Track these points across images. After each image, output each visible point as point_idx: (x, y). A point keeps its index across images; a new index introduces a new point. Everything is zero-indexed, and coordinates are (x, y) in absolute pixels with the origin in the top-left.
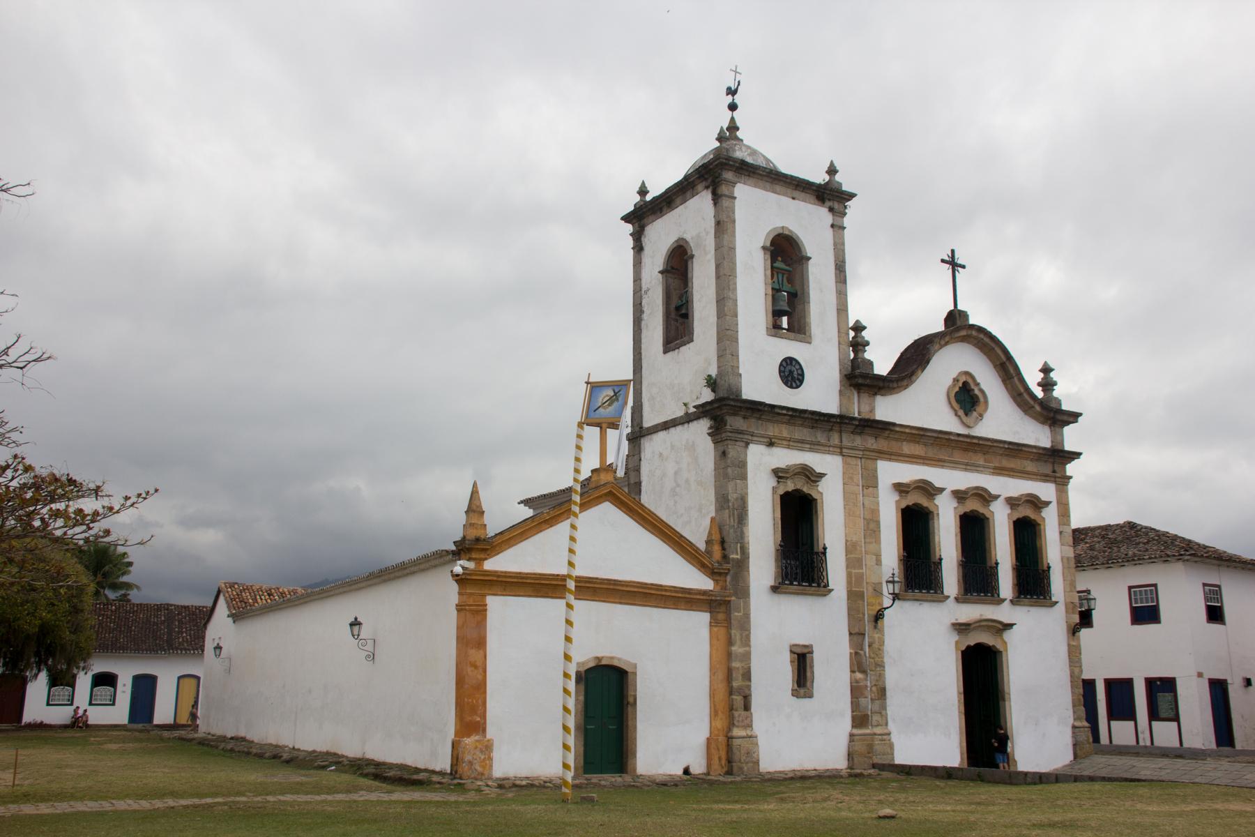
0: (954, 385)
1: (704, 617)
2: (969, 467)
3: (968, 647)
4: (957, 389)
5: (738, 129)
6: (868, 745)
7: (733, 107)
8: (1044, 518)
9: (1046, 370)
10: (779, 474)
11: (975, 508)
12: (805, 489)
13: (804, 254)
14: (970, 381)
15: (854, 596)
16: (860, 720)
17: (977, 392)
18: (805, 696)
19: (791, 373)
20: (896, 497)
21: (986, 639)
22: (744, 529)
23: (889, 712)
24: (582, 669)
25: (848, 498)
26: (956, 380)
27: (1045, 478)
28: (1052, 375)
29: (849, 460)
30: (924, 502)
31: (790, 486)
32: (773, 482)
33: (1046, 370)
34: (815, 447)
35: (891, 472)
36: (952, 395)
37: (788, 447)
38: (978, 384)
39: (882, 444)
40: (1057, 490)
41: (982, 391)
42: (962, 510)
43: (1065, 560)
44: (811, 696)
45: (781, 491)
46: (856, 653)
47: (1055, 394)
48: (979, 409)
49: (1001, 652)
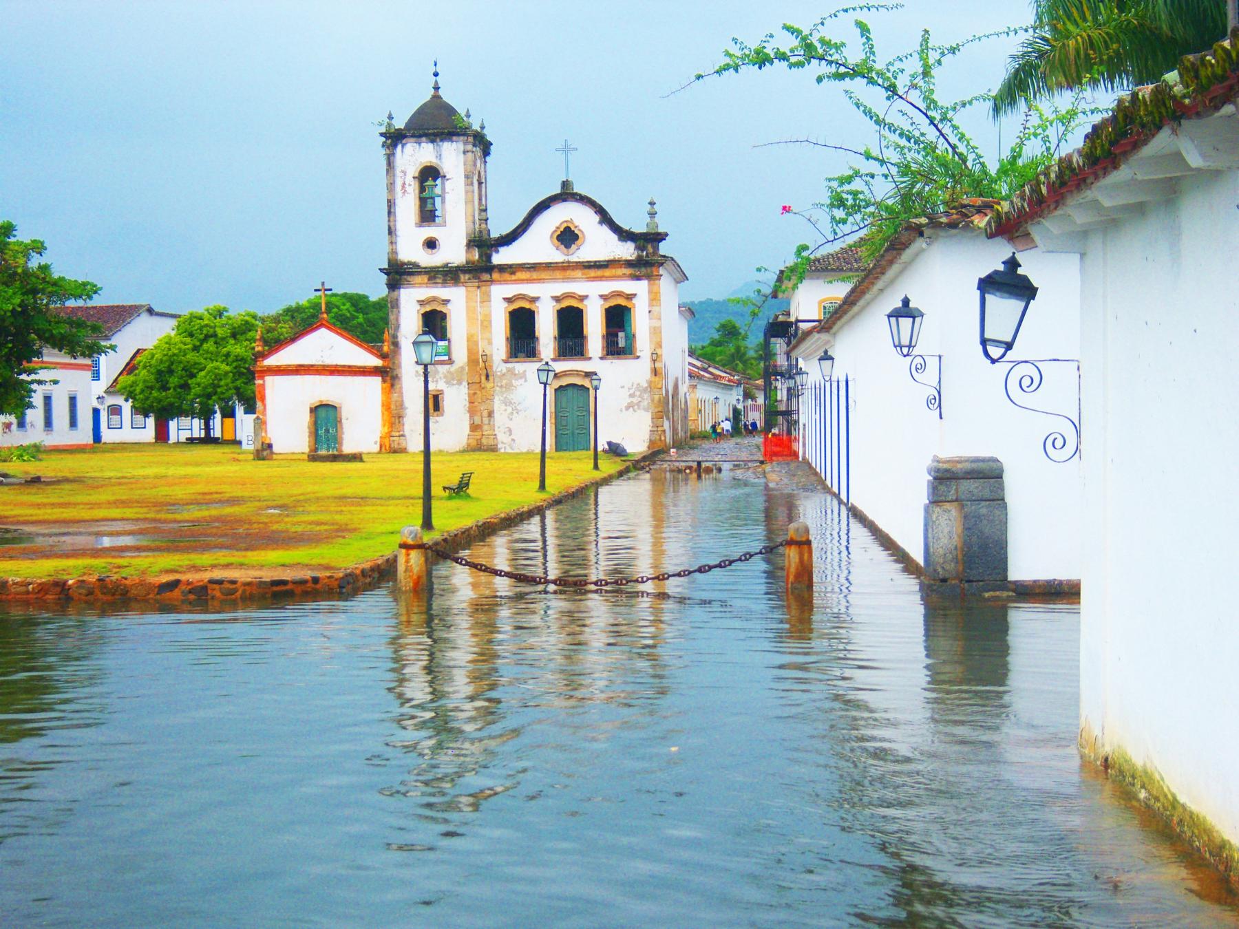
0: (555, 231)
1: (379, 379)
2: (566, 279)
3: (561, 387)
4: (559, 233)
5: (439, 88)
6: (477, 440)
7: (436, 74)
8: (634, 304)
9: (652, 204)
10: (422, 303)
11: (569, 304)
12: (438, 309)
13: (442, 174)
14: (570, 225)
15: (473, 361)
16: (474, 428)
17: (576, 232)
18: (437, 416)
19: (431, 244)
20: (506, 304)
21: (579, 381)
22: (399, 334)
23: (497, 425)
24: (313, 406)
25: (470, 310)
26: (558, 228)
27: (638, 278)
28: (655, 206)
29: (469, 289)
30: (527, 305)
31: (428, 308)
32: (419, 307)
33: (652, 204)
34: (444, 283)
35: (501, 293)
36: (555, 236)
37: (427, 287)
38: (576, 227)
39: (496, 276)
40: (649, 285)
41: (580, 230)
42: (559, 306)
43: (652, 330)
44: (442, 415)
45: (423, 311)
46: (475, 394)
47: (656, 220)
48: (578, 242)
49: (588, 389)
